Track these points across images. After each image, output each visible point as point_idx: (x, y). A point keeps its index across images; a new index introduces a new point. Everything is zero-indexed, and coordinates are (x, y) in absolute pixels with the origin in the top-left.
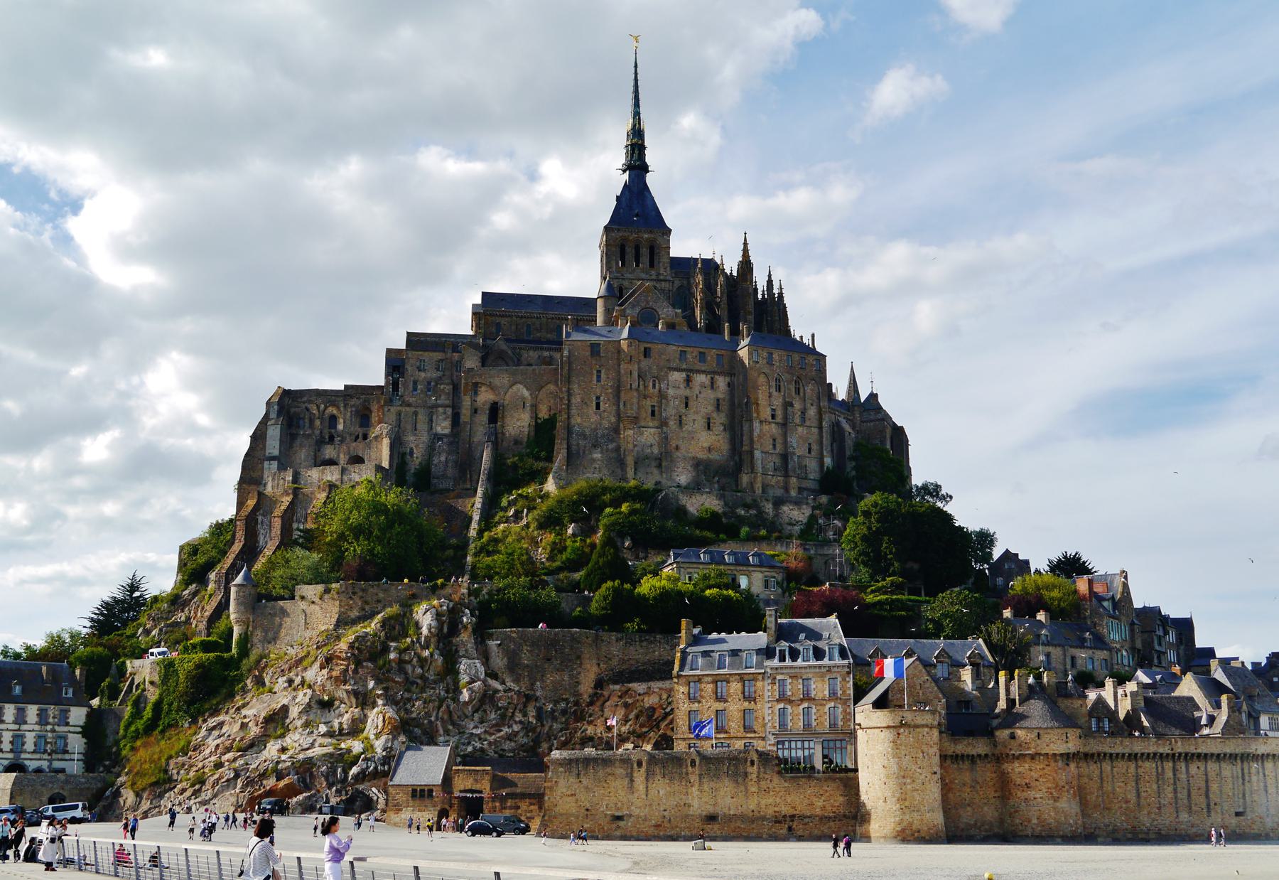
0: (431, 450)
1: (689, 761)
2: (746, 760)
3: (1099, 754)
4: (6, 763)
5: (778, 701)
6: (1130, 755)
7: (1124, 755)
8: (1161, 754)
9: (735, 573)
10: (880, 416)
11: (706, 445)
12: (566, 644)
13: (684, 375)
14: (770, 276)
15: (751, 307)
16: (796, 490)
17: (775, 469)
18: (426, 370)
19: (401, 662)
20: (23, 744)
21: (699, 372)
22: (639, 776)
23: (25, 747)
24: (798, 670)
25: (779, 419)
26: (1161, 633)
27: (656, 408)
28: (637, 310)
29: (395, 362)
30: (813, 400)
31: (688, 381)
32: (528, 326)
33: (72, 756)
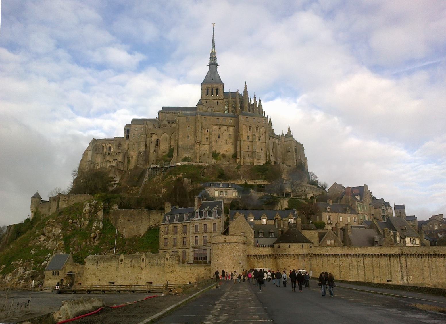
1: (142, 259)
2: (165, 259)
3: (321, 255)
5: (194, 233)
6: (336, 255)
7: (332, 255)
8: (351, 254)
9: (222, 190)
10: (290, 139)
11: (225, 150)
12: (136, 215)
13: (218, 127)
15: (247, 106)
17: (249, 157)
18: (137, 130)
19: (73, 223)
22: (121, 265)
24: (202, 221)
25: (251, 139)
29: (128, 130)
30: (263, 134)
31: (220, 128)
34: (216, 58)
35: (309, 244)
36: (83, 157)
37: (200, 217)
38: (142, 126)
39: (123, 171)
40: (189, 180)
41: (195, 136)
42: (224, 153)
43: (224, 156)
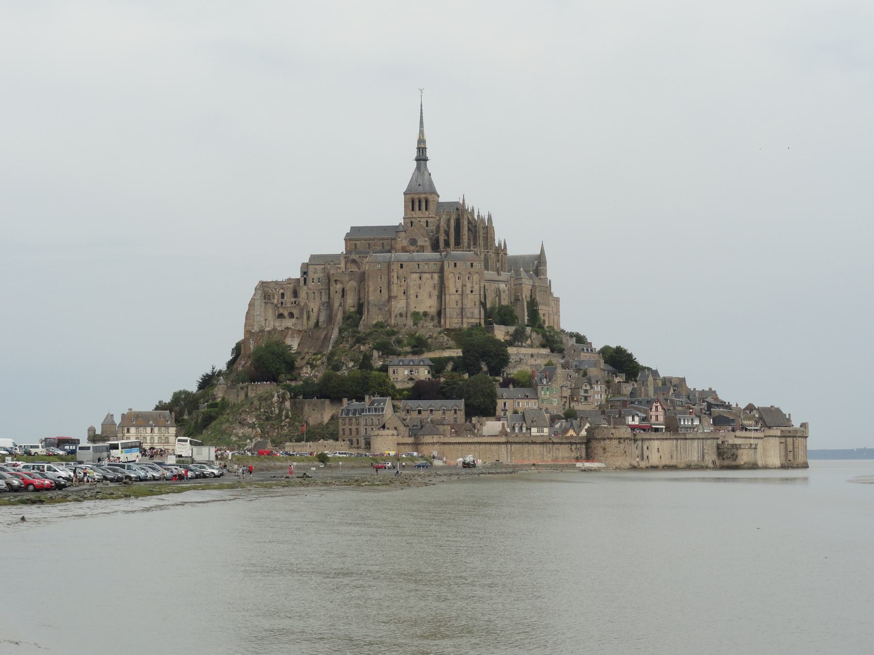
0: (319, 309)
4: (149, 447)
11: (429, 305)
13: (418, 275)
14: (479, 213)
16: (466, 324)
17: (457, 315)
19: (264, 412)
20: (154, 440)
21: (425, 273)
23: (155, 441)
25: (460, 292)
26: (588, 387)
27: (406, 291)
28: (408, 240)
31: (420, 278)
32: (369, 244)
33: (171, 444)
34: (426, 148)
35: (438, 436)
36: (249, 307)
37: (369, 412)
38: (323, 267)
39: (301, 331)
40: (379, 352)
41: (389, 290)
42: (426, 310)
43: (425, 314)
